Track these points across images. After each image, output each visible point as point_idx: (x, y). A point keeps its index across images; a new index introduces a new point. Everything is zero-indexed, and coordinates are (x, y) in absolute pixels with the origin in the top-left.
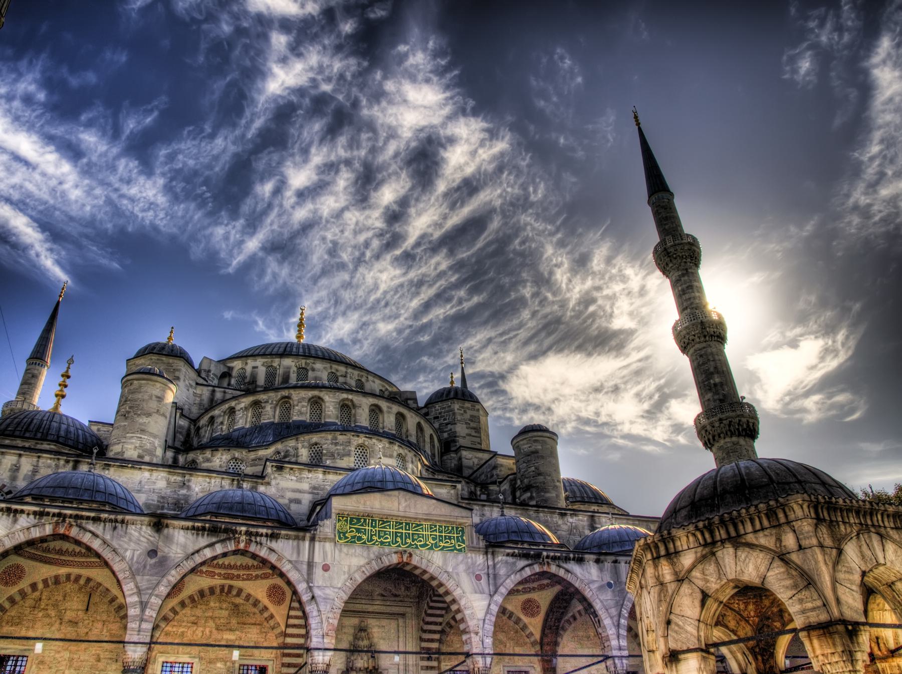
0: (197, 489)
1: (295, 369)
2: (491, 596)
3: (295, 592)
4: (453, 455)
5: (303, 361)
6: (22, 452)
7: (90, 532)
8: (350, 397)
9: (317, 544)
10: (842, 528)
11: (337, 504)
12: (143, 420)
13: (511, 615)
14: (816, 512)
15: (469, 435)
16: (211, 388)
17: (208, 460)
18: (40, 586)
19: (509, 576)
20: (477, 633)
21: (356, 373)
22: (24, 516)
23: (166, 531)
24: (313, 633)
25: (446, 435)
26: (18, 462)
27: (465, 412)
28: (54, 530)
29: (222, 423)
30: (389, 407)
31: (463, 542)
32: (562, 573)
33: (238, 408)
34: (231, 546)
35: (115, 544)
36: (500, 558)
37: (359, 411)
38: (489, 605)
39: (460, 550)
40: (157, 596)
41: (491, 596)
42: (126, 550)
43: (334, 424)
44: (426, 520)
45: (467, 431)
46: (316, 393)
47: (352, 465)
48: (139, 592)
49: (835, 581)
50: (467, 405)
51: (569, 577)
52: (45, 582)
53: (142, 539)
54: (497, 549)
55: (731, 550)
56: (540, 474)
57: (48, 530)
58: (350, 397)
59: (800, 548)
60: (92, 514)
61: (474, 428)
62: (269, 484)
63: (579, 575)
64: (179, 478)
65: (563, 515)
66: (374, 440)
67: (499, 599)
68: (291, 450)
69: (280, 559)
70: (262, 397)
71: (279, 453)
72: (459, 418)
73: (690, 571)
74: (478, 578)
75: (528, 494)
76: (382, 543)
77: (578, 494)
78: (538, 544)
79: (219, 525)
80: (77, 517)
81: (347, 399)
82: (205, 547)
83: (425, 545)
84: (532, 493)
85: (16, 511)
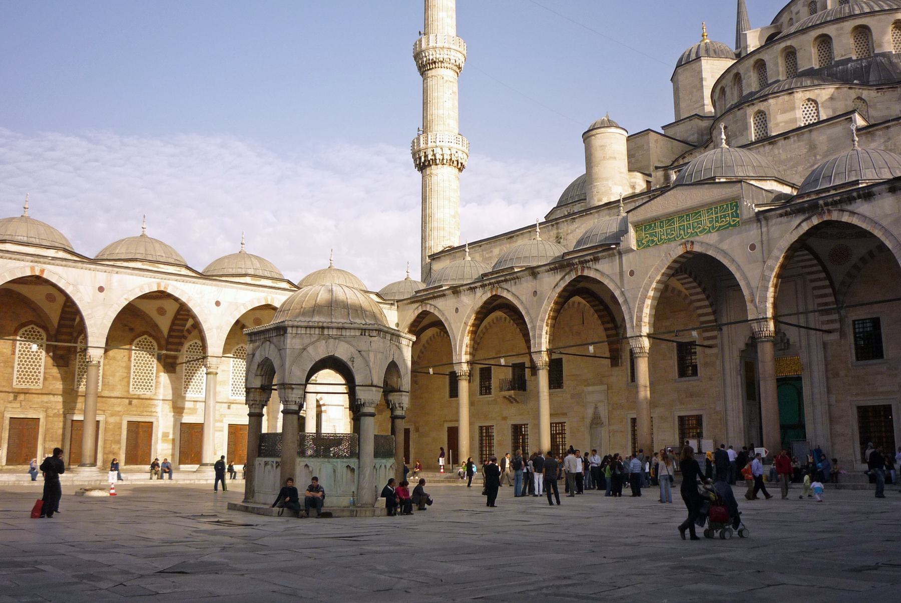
2: (764, 262)
8: (789, 43)
9: (624, 258)
23: (539, 276)
30: (837, 30)
31: (737, 217)
32: (846, 218)
34: (573, 276)
36: (774, 221)
37: (799, 55)
38: (763, 271)
39: (735, 226)
51: (855, 221)
57: (489, 295)
58: (789, 43)
60: (503, 278)
63: (867, 214)
66: (771, 101)
69: (603, 274)
70: (724, 82)
74: (753, 247)
80: (498, 282)
81: (787, 47)
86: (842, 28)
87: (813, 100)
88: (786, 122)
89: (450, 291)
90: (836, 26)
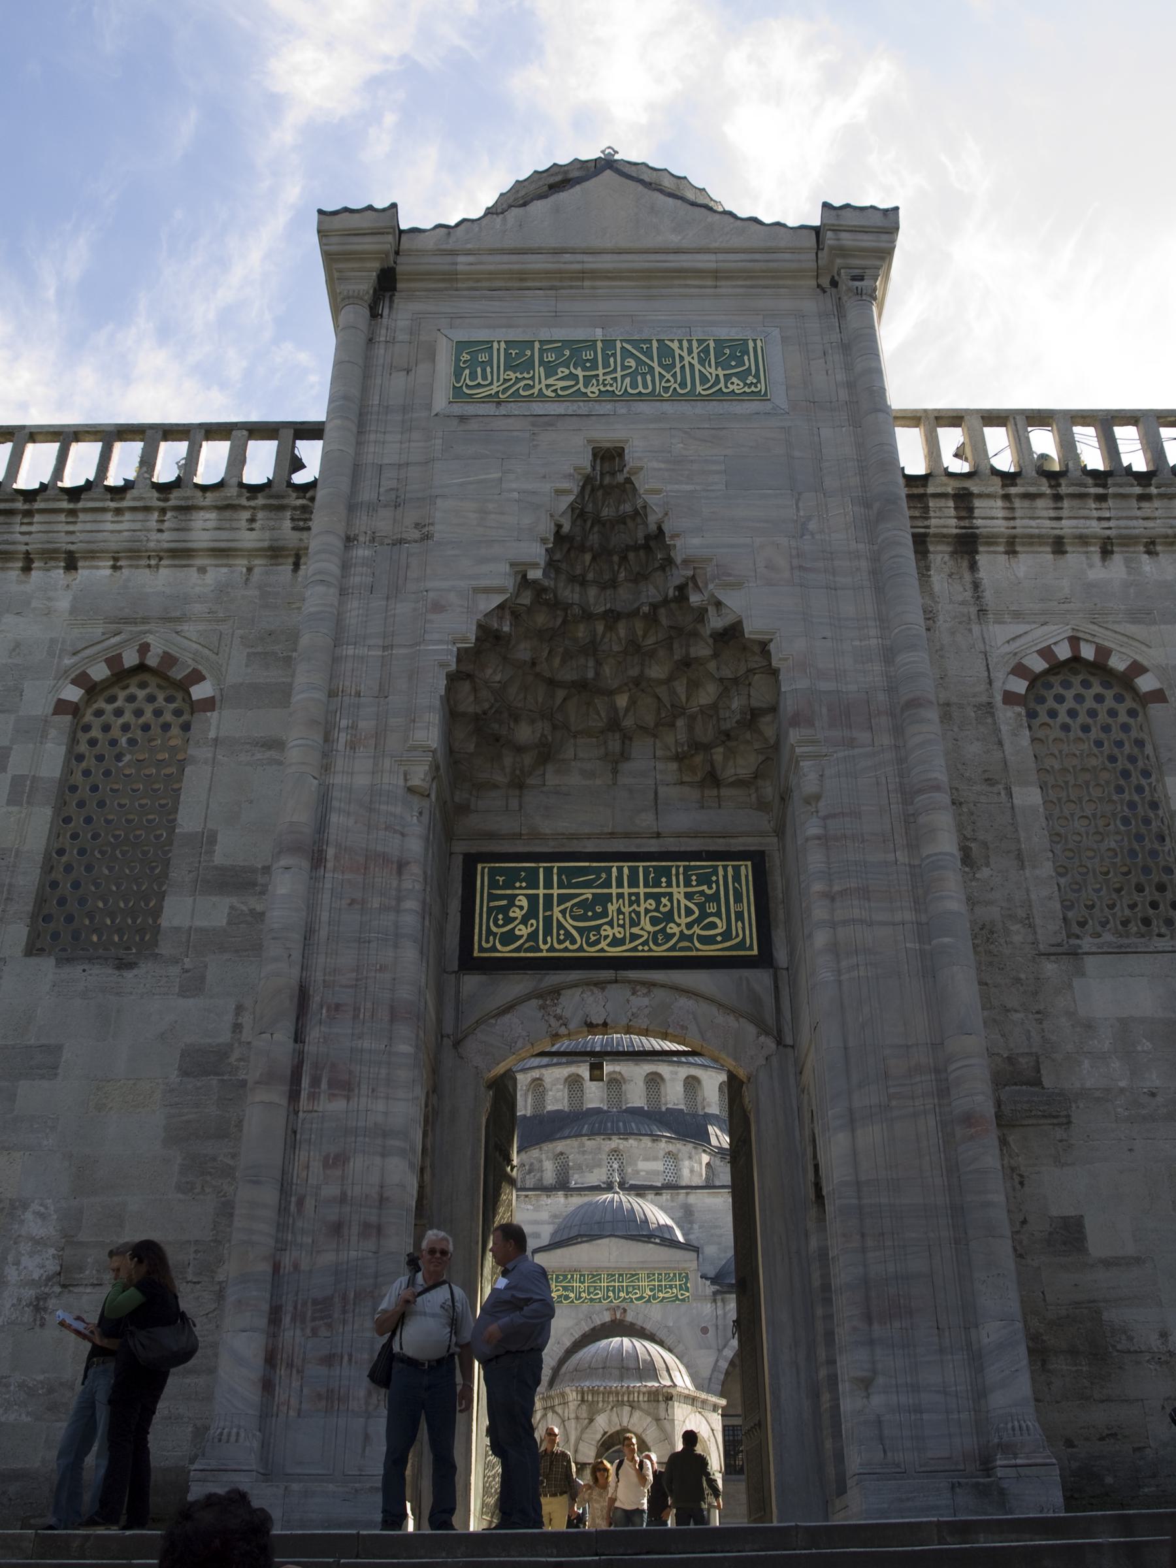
2: (720, 1351)
8: (617, 1068)
10: (600, 1405)
14: (583, 1397)
30: (671, 1072)
31: (687, 1290)
38: (717, 1361)
41: (720, 1351)
43: (598, 1111)
44: (642, 1269)
47: (604, 1178)
49: (579, 1439)
54: (728, 1296)
58: (617, 1068)
66: (631, 1141)
74: (705, 1330)
76: (592, 1300)
81: (614, 1072)
83: (641, 1298)
86: (676, 1073)
88: (648, 1172)
90: (671, 1068)
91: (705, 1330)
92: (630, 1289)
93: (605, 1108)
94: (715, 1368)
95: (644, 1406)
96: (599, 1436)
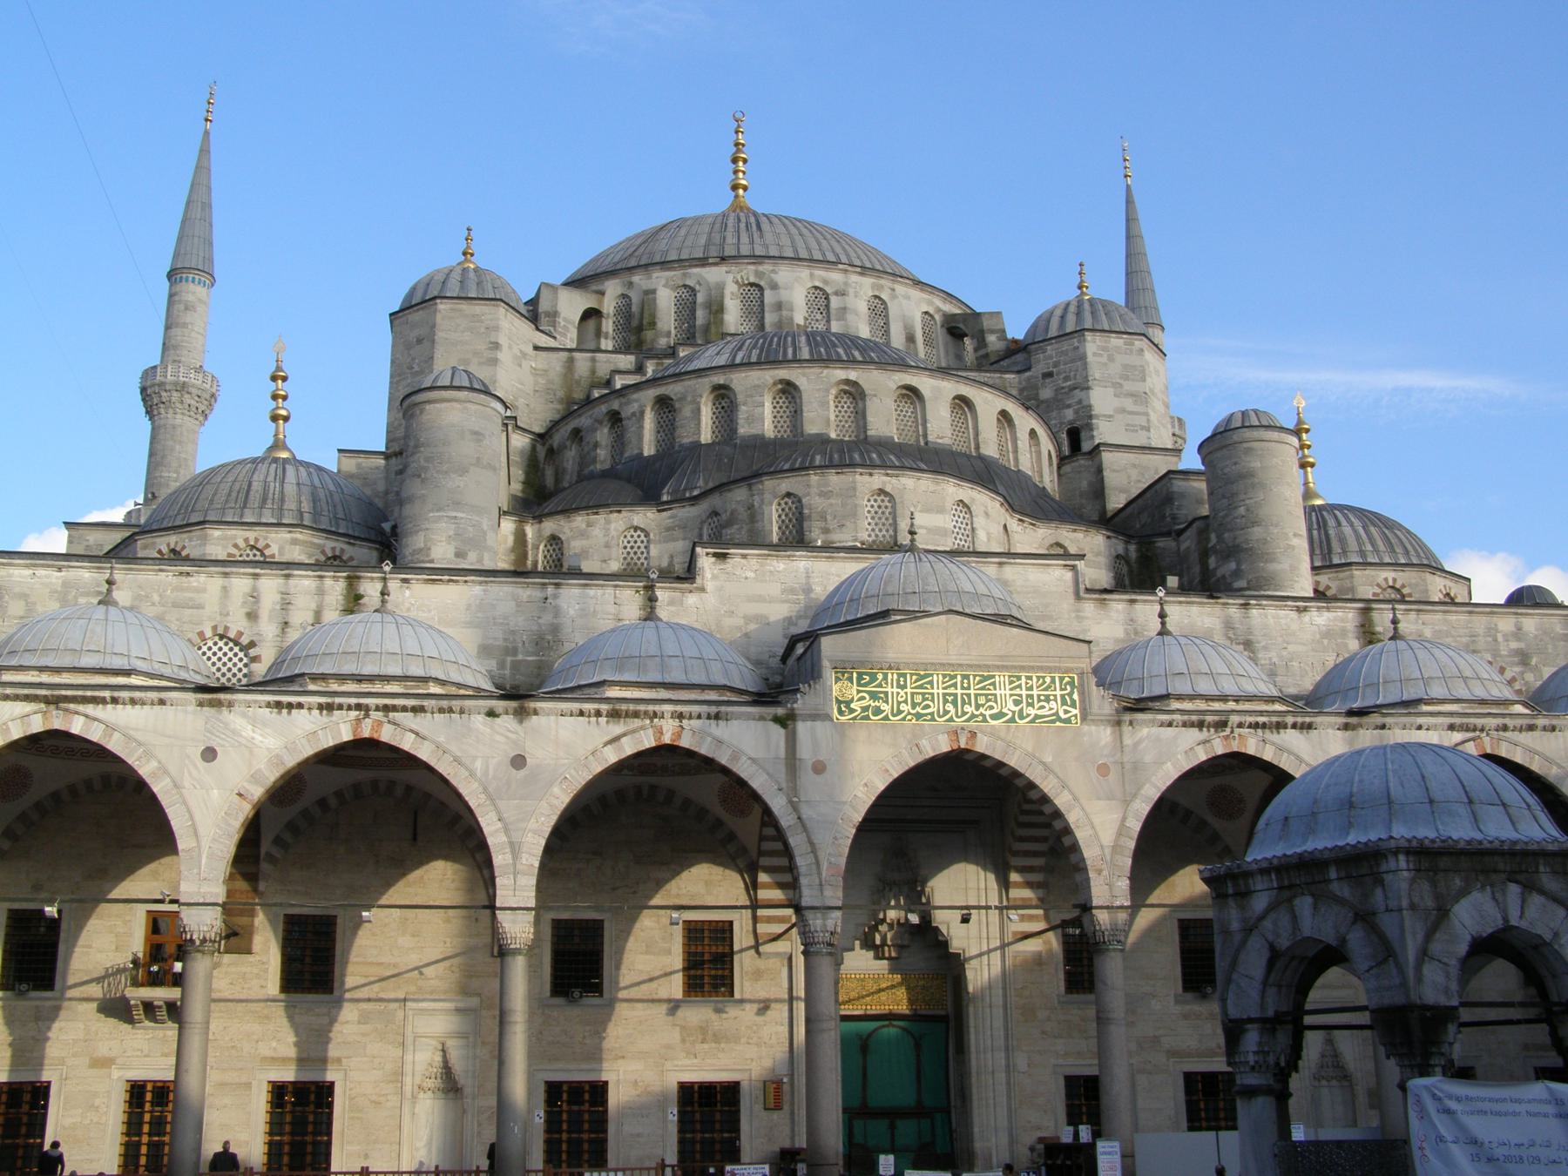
0: (572, 612)
1: (734, 288)
2: (1127, 802)
3: (767, 811)
4: (1082, 461)
5: (752, 267)
6: (258, 571)
7: (412, 731)
8: (853, 375)
9: (802, 728)
11: (830, 646)
12: (456, 481)
13: (1188, 813)
15: (1123, 411)
16: (565, 354)
17: (583, 534)
18: (333, 802)
19: (1159, 763)
20: (1099, 872)
21: (867, 281)
22: (304, 712)
24: (803, 881)
25: (1069, 414)
26: (255, 589)
27: (1111, 359)
28: (354, 733)
29: (596, 445)
31: (1073, 705)
32: (1268, 755)
33: (623, 415)
34: (648, 742)
35: (453, 748)
36: (1145, 731)
38: (1124, 819)
40: (535, 832)
42: (475, 758)
43: (823, 441)
45: (1117, 402)
46: (783, 373)
47: (864, 536)
48: (506, 830)
49: (1424, 954)
50: (1116, 341)
52: (339, 794)
53: (498, 738)
54: (1140, 716)
55: (1308, 900)
56: (1254, 523)
57: (346, 736)
59: (1387, 910)
61: (1132, 395)
62: (702, 590)
64: (537, 594)
65: (1299, 610)
66: (904, 480)
67: (1143, 808)
68: (741, 510)
69: (735, 756)
70: (673, 389)
71: (715, 513)
72: (1097, 376)
73: (1262, 918)
74: (1103, 770)
75: (1233, 565)
76: (918, 716)
77: (1353, 545)
78: (1224, 698)
79: (624, 707)
82: (606, 744)
83: (1000, 715)
84: (1238, 564)
85: (290, 706)
87: (965, 505)
88: (929, 530)
89: (191, 696)
91: (1103, 770)
92: (982, 700)
93: (833, 436)
94: (1122, 830)
95: (1548, 881)
96: (1462, 948)
